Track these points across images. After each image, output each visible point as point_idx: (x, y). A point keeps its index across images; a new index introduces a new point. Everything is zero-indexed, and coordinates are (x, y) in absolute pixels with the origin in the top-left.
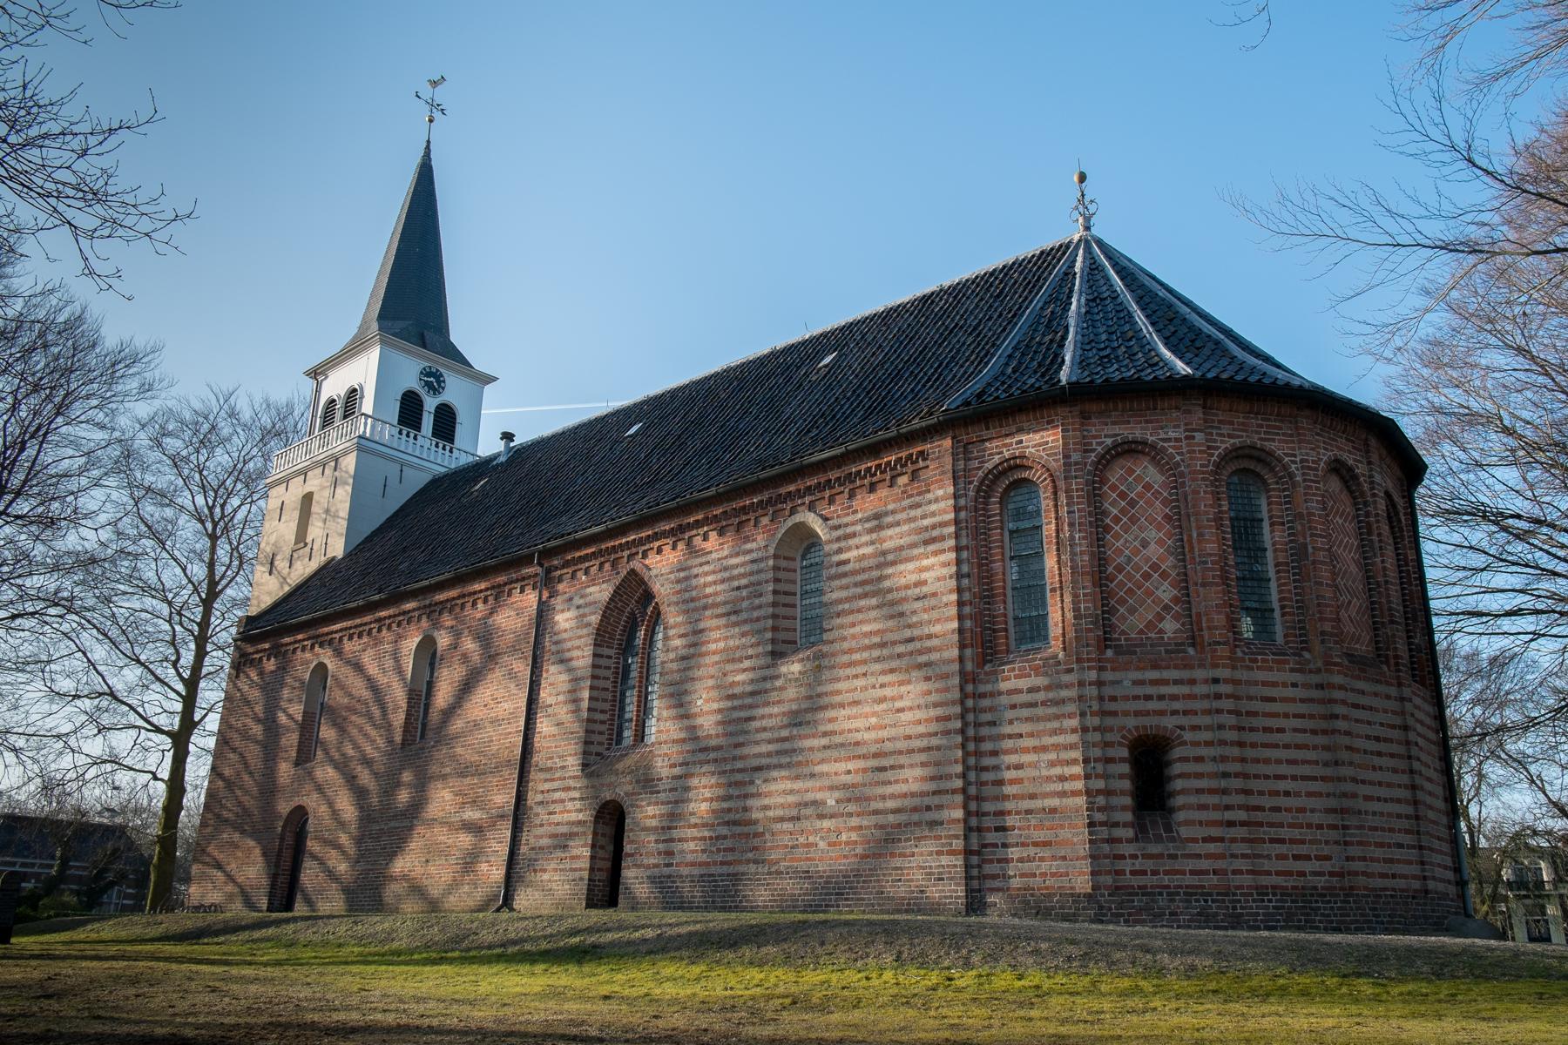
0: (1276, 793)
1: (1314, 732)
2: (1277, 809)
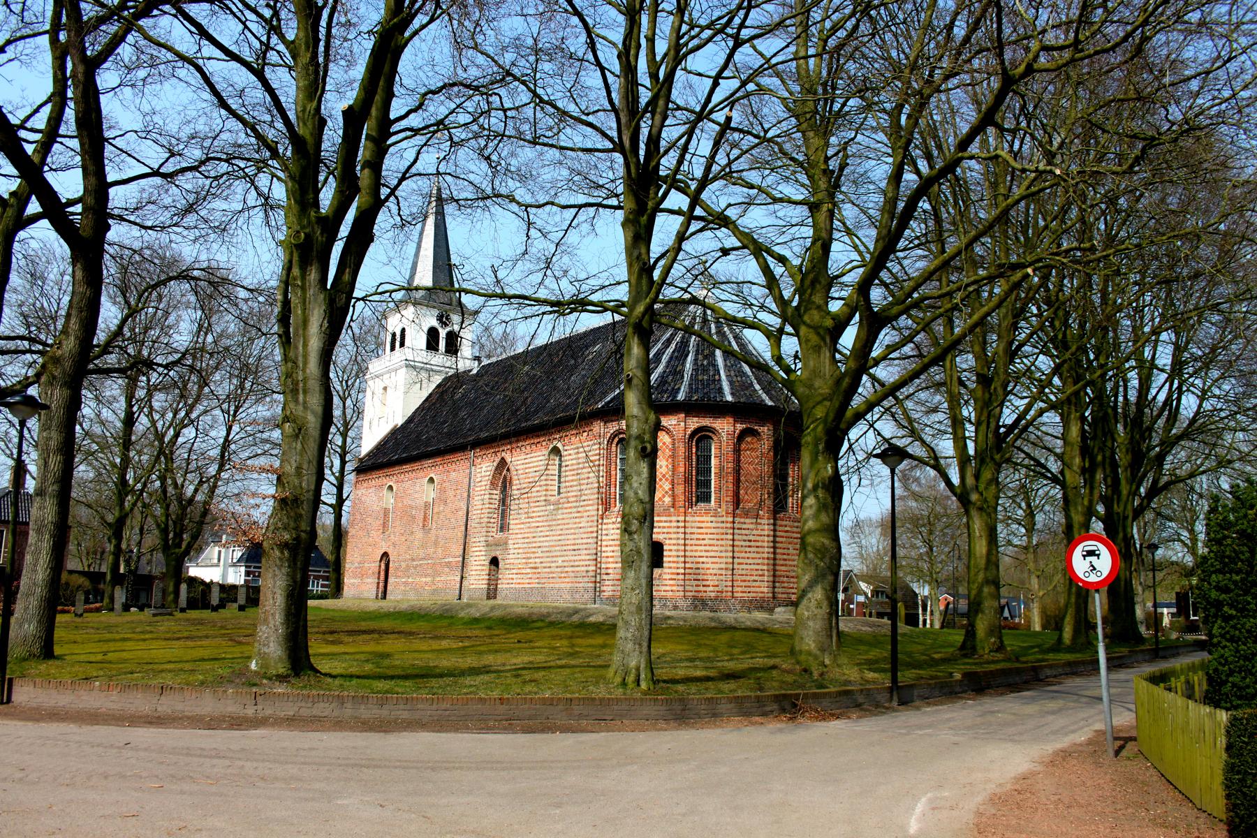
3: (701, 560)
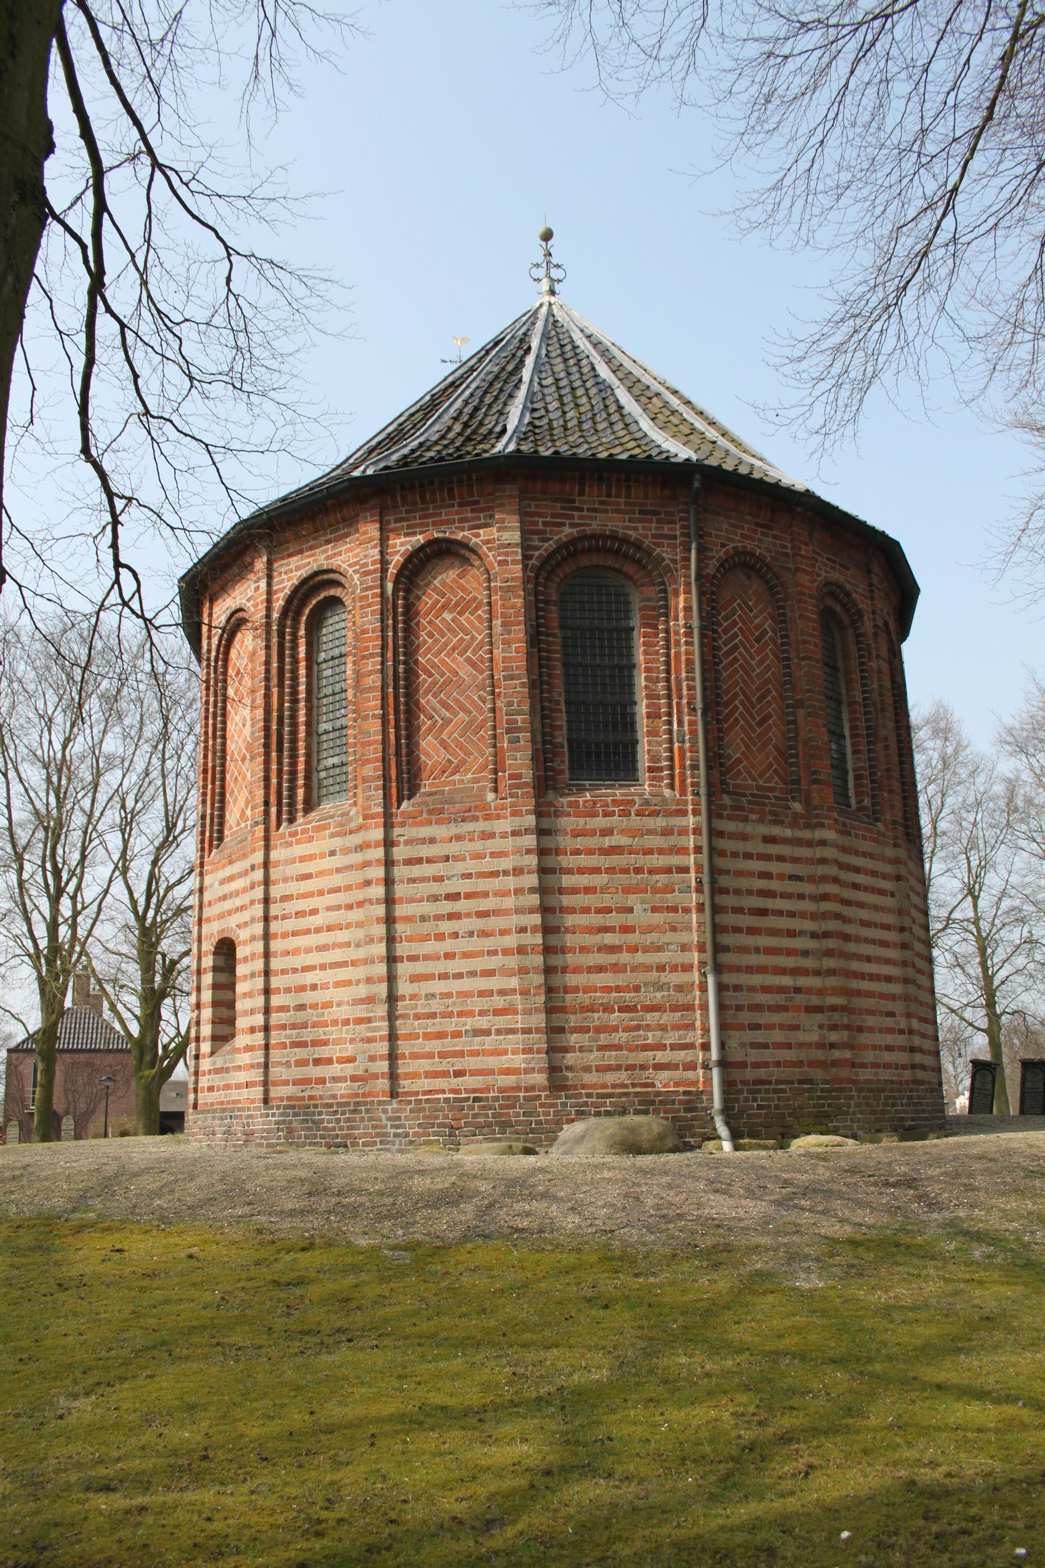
0: (301, 989)
1: (349, 907)
2: (301, 1007)
3: (310, 978)
